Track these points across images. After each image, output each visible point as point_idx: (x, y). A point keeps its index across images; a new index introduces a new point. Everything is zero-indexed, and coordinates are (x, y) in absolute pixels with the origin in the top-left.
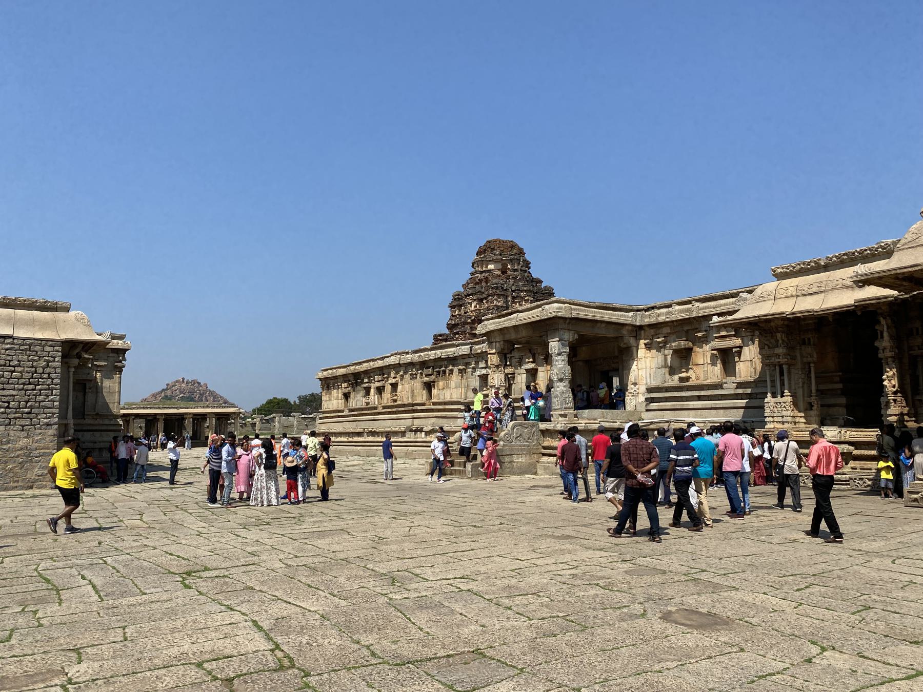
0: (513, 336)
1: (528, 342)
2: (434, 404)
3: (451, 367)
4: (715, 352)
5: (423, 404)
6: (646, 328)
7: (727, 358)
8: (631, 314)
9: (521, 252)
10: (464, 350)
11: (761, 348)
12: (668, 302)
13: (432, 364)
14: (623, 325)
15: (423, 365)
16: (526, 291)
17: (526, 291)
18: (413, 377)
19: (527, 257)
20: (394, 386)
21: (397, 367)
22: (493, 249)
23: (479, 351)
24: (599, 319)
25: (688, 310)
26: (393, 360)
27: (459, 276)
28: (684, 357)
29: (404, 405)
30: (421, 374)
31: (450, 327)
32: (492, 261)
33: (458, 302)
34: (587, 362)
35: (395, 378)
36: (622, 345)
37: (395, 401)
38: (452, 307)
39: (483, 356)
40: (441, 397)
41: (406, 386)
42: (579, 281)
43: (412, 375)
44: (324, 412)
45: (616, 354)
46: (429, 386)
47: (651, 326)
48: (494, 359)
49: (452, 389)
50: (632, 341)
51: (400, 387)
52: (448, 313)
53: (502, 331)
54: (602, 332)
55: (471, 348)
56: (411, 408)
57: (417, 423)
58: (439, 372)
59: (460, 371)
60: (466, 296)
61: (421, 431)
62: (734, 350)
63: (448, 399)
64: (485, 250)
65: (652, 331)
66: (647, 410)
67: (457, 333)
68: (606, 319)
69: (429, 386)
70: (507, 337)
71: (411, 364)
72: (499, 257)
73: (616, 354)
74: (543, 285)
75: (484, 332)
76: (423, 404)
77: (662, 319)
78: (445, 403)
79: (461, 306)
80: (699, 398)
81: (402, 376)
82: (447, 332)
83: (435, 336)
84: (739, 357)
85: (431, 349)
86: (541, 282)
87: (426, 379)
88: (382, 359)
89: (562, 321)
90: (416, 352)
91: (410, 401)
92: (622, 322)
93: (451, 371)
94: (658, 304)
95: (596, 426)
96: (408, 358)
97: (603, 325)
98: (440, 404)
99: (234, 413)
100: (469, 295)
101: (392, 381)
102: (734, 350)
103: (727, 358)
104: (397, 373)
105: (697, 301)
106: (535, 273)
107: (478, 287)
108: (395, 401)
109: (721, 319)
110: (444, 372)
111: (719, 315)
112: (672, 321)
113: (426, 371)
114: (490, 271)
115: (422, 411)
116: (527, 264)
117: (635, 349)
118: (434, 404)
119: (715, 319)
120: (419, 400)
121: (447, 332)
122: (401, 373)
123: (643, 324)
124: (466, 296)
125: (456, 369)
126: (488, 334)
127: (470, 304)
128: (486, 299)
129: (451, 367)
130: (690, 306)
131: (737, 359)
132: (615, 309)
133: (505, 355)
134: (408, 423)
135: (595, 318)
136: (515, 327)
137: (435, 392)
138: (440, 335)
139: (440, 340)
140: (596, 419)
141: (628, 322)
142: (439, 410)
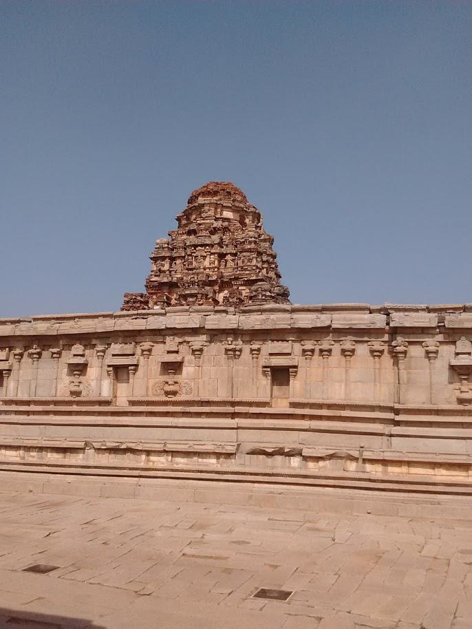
20: (172, 368)
51: (188, 370)
55: (442, 320)
69: (281, 375)
79: (172, 259)
91: (222, 395)
114: (228, 220)
127: (204, 257)
139: (135, 303)
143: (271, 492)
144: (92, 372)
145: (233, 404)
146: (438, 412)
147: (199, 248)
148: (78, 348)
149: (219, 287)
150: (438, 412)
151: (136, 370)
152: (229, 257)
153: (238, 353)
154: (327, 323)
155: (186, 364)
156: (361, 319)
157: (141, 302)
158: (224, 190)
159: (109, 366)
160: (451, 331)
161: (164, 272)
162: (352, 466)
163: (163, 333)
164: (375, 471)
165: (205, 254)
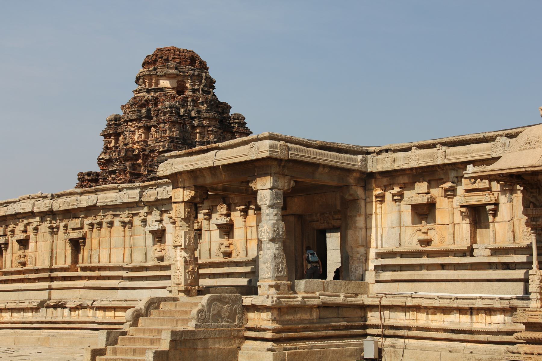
0: (208, 180)
1: (225, 189)
2: (83, 269)
4: (464, 209)
6: (378, 177)
7: (478, 216)
8: (360, 157)
9: (203, 67)
10: (132, 196)
11: (527, 204)
12: (406, 145)
14: (349, 171)
16: (209, 119)
17: (209, 119)
19: (212, 73)
22: (167, 60)
23: (152, 199)
24: (321, 162)
25: (433, 156)
27: (119, 92)
28: (424, 212)
29: (37, 271)
30: (66, 226)
31: (102, 163)
32: (166, 76)
33: (114, 129)
34: (300, 217)
36: (347, 197)
38: (106, 136)
39: (163, 205)
42: (277, 106)
45: (338, 208)
47: (384, 174)
48: (179, 211)
49: (109, 247)
50: (360, 192)
52: (100, 143)
53: (194, 174)
54: (323, 178)
57: (56, 296)
58: (92, 225)
59: (124, 224)
60: (127, 122)
61: (63, 306)
62: (488, 207)
63: (104, 262)
64: (155, 62)
65: (385, 181)
66: (377, 281)
67: (114, 172)
68: (330, 163)
69: (77, 245)
70: (200, 181)
72: (175, 71)
73: (338, 208)
74: (232, 112)
75: (168, 173)
77: (398, 165)
78: (100, 269)
80: (443, 267)
82: (97, 169)
83: (80, 174)
84: (495, 215)
85: (82, 194)
86: (229, 107)
89: (275, 163)
92: (349, 167)
93: (111, 224)
94: (393, 146)
95: (317, 301)
97: (327, 170)
100: (131, 121)
102: (488, 207)
103: (478, 216)
105: (444, 144)
106: (221, 93)
107: (143, 109)
109: (477, 169)
111: (474, 163)
112: (411, 169)
114: (161, 89)
115: (65, 279)
116: (211, 83)
117: (362, 203)
118: (83, 269)
119: (470, 168)
120: (60, 263)
121: (97, 169)
123: (374, 170)
124: (127, 122)
125: (117, 222)
126: (175, 179)
127: (133, 132)
128: (155, 126)
130: (434, 150)
131: (491, 218)
132: (340, 150)
133: (196, 204)
134: (44, 296)
135: (317, 161)
136: (213, 169)
137: (85, 253)
138: (89, 174)
139: (89, 181)
140: (314, 292)
141: (356, 168)
143: (49, 335)
144: (441, 216)
146: (146, 269)
147: (130, 123)
148: (422, 186)
149: (143, 160)
150: (146, 269)
151: (84, 243)
152: (153, 129)
153: (55, 230)
155: (31, 241)
156: (111, 197)
157: (89, 180)
158: (162, 57)
159: (462, 206)
160: (149, 204)
161: (111, 148)
163: (18, 216)
165: (133, 129)
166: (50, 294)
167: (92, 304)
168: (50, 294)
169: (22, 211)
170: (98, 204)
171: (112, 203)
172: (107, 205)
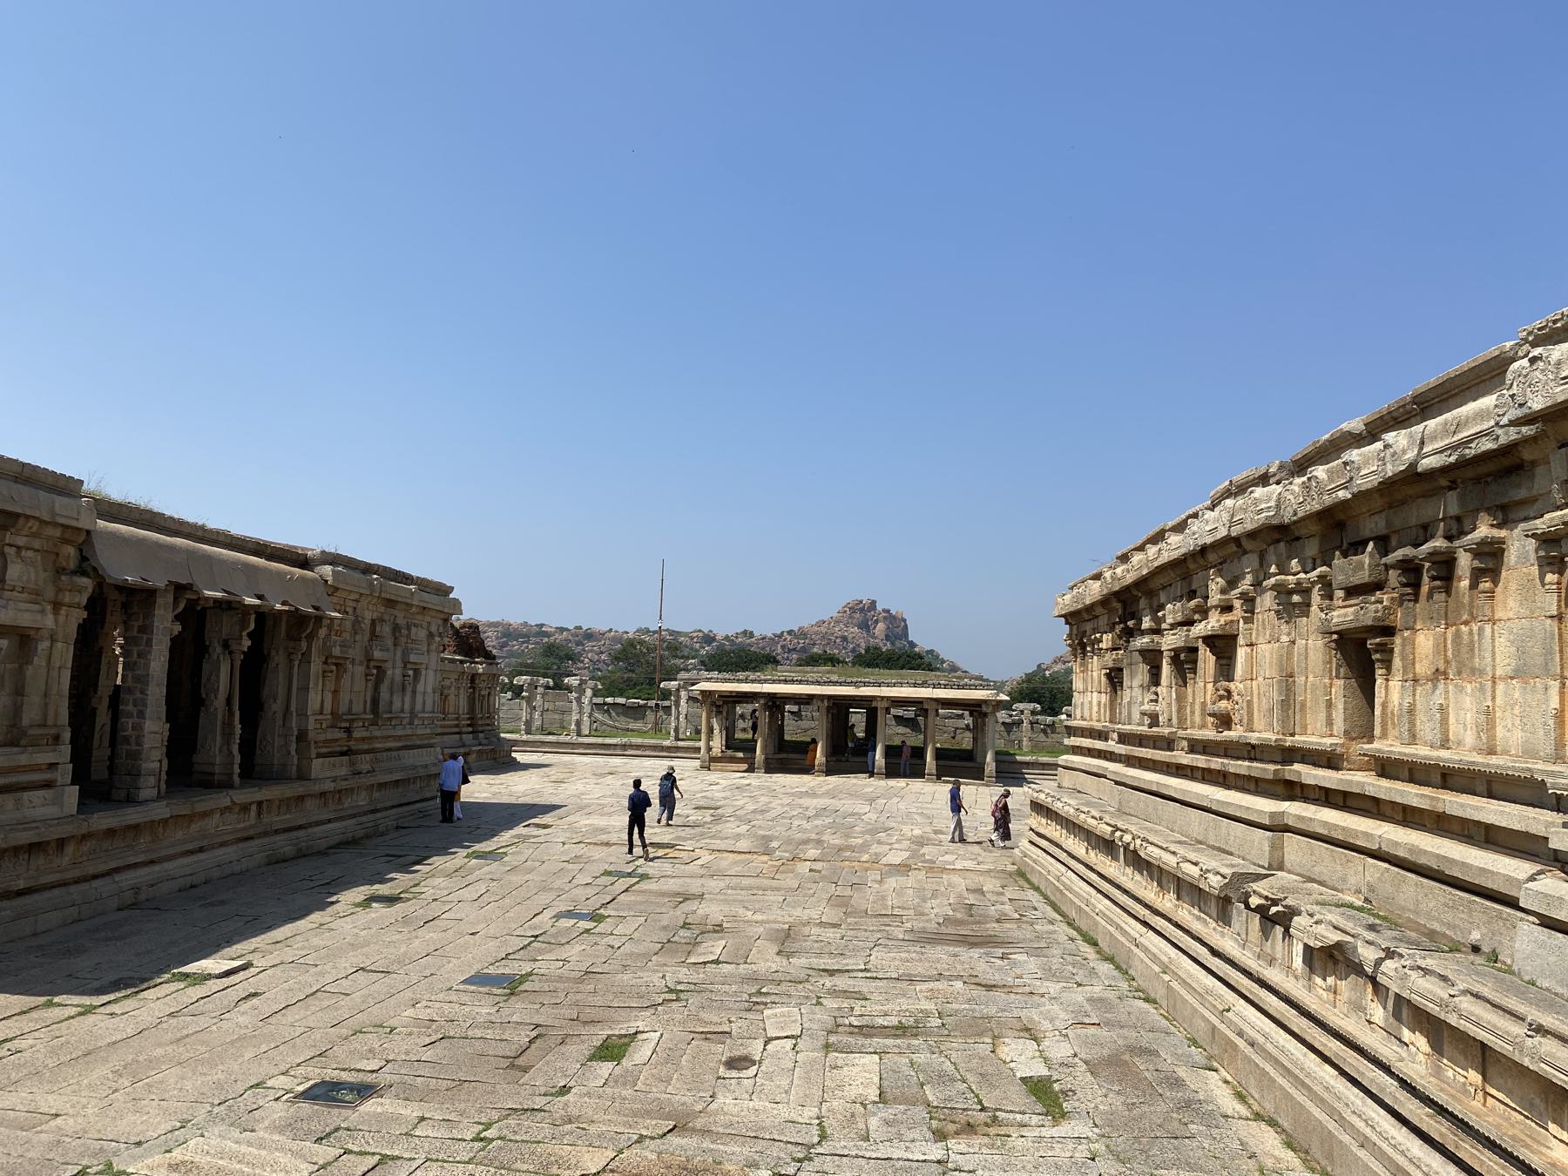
2: (1386, 767)
3: (1484, 530)
5: (1330, 760)
13: (1374, 525)
15: (1335, 528)
18: (1292, 605)
21: (1224, 553)
26: (1211, 526)
35: (1228, 608)
37: (1225, 721)
40: (1427, 727)
41: (1265, 650)
43: (1282, 591)
44: (1072, 732)
46: (1361, 655)
56: (1277, 770)
58: (1411, 570)
69: (1361, 655)
71: (1278, 537)
76: (1330, 760)
81: (1249, 601)
87: (1345, 614)
88: (1180, 528)
90: (1300, 466)
93: (1491, 558)
96: (1264, 504)
98: (1414, 772)
99: (986, 701)
101: (1213, 623)
104: (1232, 584)
108: (1225, 721)
110: (1445, 567)
113: (1345, 570)
118: (1386, 767)
122: (1246, 584)
125: (1520, 547)
129: (1484, 530)
137: (1391, 691)
142: (1407, 816)
145: (1291, 755)
153: (1296, 598)
154: (1411, 455)
156: (1481, 415)
162: (1378, 1013)
164: (1414, 1055)
166: (1276, 847)
167: (1379, 962)
168: (1276, 847)
169: (1209, 540)
170: (1427, 463)
171: (1487, 445)
172: (1463, 464)
